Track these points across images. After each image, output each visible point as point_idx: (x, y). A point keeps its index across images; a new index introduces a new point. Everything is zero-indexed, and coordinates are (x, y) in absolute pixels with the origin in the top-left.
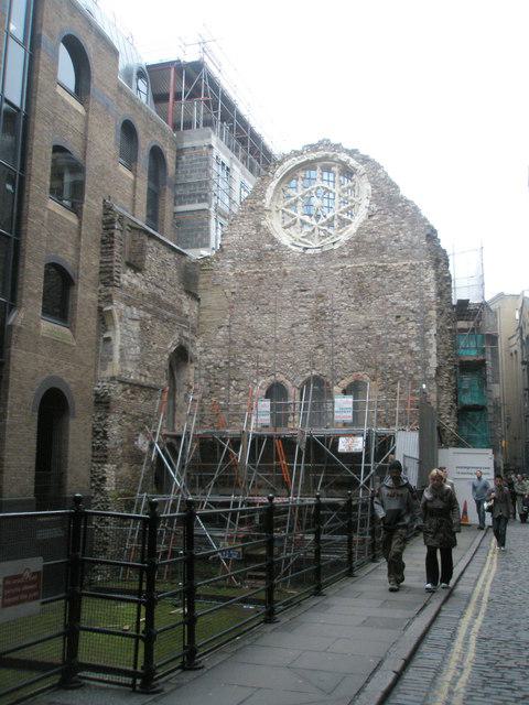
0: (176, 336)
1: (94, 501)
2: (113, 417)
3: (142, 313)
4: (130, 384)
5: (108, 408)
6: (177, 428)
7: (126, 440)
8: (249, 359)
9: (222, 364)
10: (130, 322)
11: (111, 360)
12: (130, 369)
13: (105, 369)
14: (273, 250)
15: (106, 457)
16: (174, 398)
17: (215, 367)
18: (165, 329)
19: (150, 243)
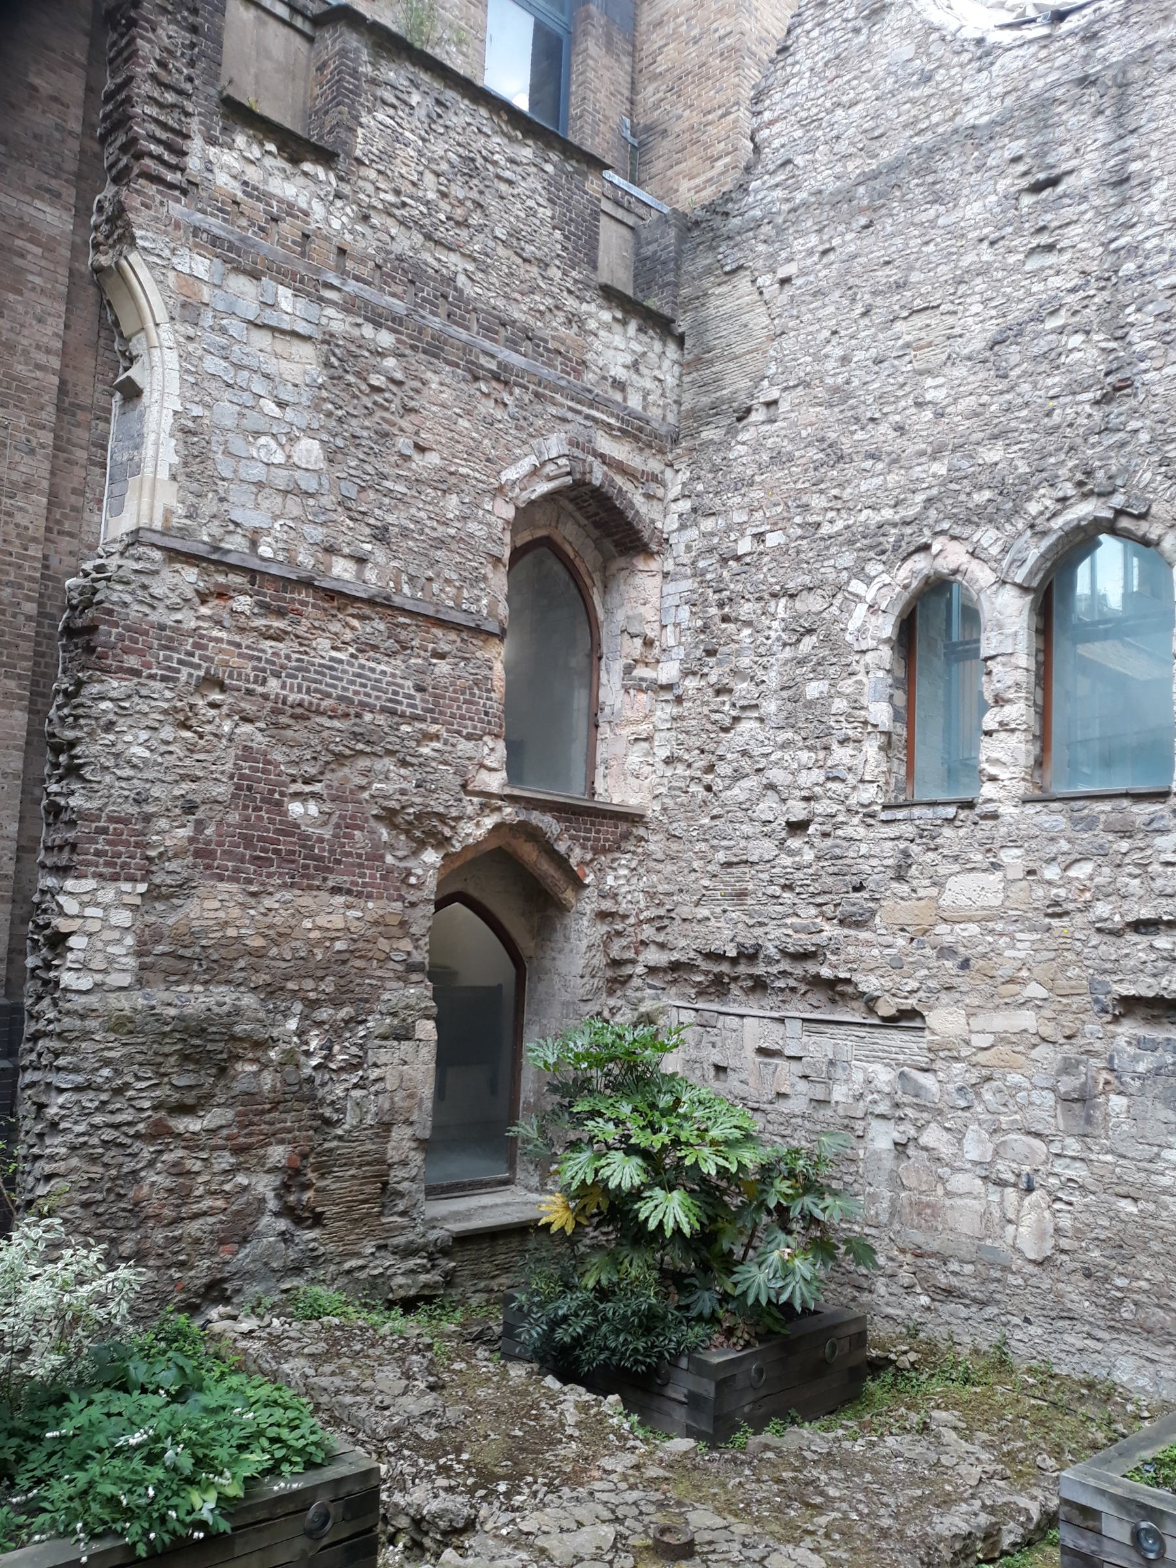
0: (555, 444)
1: (30, 1028)
2: (116, 685)
3: (338, 322)
4: (252, 573)
5: (90, 650)
6: (599, 786)
7: (222, 790)
8: (839, 505)
9: (744, 546)
10: (262, 339)
11: (137, 469)
12: (251, 518)
13: (118, 510)
14: (926, 78)
15: (74, 847)
16: (593, 685)
17: (724, 561)
18: (486, 407)
19: (394, 73)
